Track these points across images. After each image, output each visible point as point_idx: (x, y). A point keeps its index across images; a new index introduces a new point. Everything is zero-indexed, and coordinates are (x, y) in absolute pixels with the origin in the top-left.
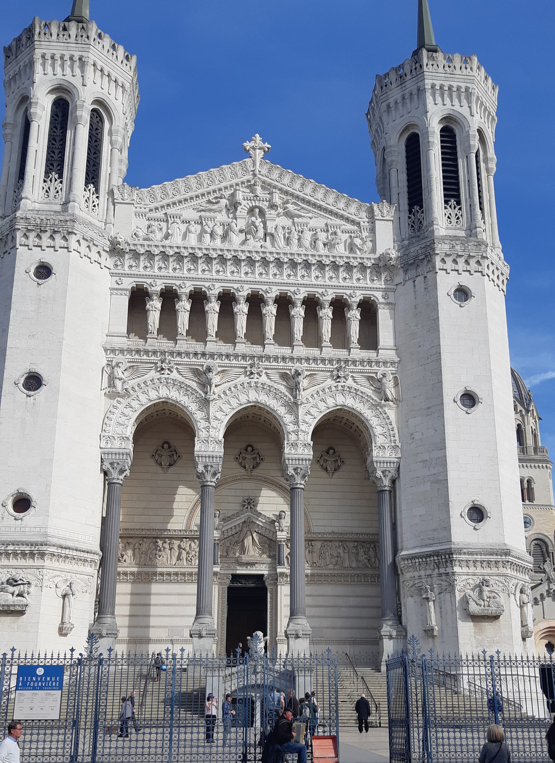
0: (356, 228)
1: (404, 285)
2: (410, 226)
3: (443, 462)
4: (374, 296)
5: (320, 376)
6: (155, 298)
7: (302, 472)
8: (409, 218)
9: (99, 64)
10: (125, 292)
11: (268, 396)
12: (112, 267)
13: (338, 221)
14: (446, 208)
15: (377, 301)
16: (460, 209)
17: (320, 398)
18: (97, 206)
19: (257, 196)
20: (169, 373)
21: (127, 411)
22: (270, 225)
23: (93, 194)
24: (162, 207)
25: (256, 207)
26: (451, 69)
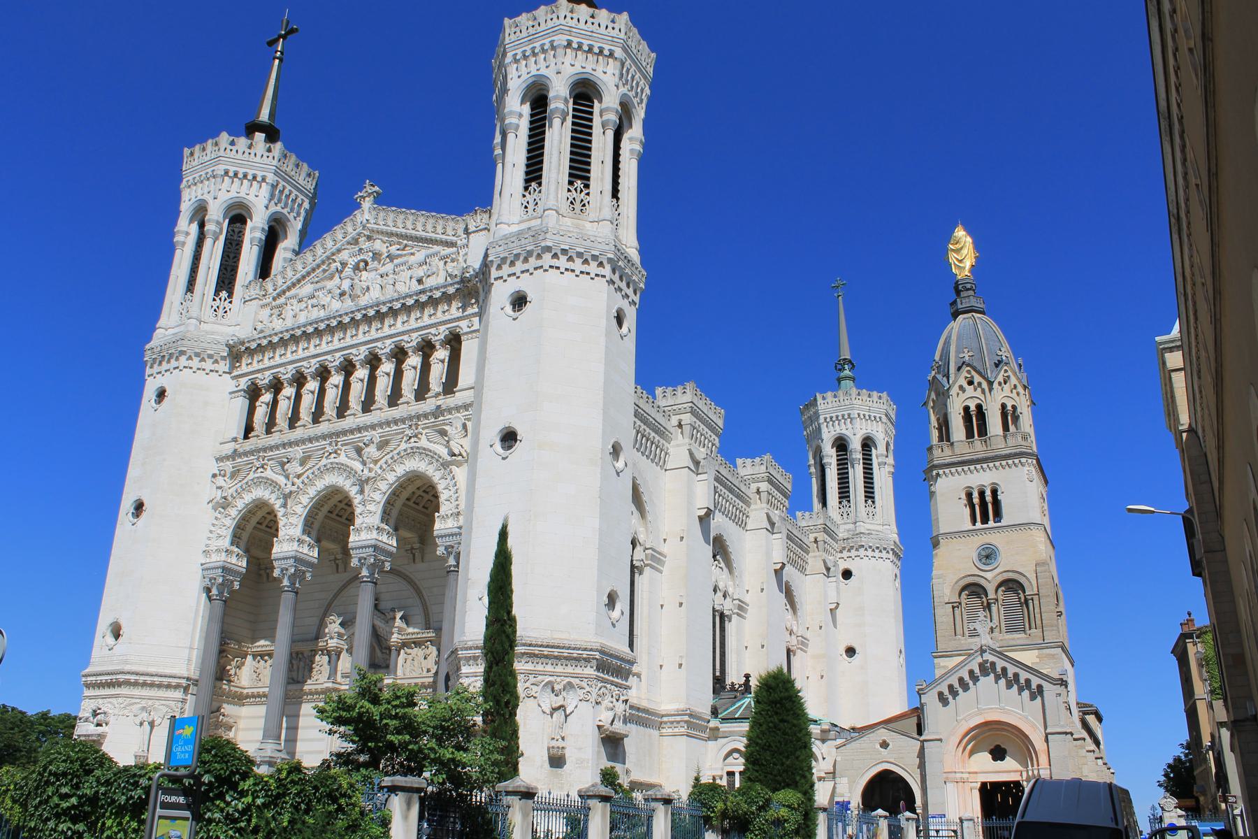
6: (264, 391)
9: (232, 170)
13: (436, 248)
14: (524, 196)
16: (540, 192)
23: (225, 300)
24: (284, 292)
26: (535, 28)
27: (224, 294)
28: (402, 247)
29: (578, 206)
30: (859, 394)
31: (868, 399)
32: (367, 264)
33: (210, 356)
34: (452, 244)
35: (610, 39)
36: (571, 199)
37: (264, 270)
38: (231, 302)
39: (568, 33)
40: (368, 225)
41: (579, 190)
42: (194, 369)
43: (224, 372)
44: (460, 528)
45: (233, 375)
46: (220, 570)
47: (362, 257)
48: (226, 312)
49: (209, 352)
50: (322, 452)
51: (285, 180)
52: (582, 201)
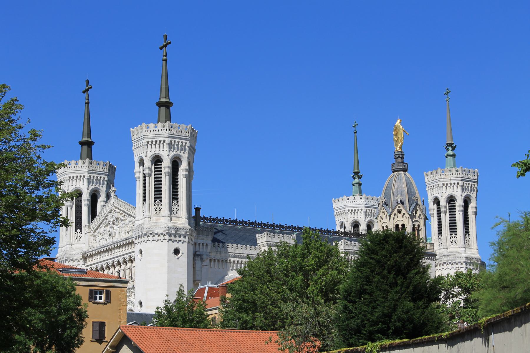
29: (158, 211)
30: (443, 172)
31: (449, 173)
33: (76, 260)
35: (163, 135)
36: (155, 209)
37: (93, 214)
38: (81, 233)
39: (147, 138)
41: (158, 204)
43: (82, 265)
45: (86, 265)
48: (80, 238)
49: (75, 258)
51: (93, 173)
52: (159, 208)
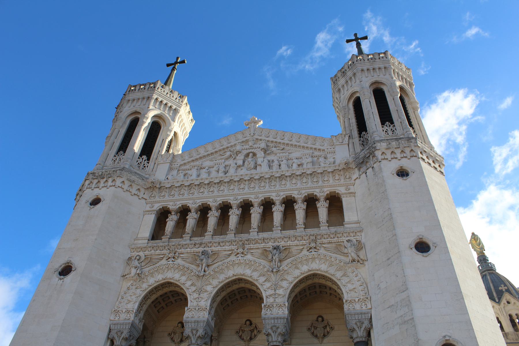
0: (321, 153)
1: (360, 178)
2: (361, 144)
3: (408, 303)
4: (338, 190)
5: (294, 250)
6: (173, 213)
7: (279, 330)
8: (360, 140)
10: (154, 212)
11: (250, 269)
12: (148, 198)
14: (383, 127)
15: (340, 192)
16: (394, 126)
17: (294, 266)
18: (146, 167)
19: (251, 146)
20: (173, 260)
21: (138, 291)
22: (259, 161)
23: (145, 161)
24: (189, 162)
25: (251, 152)
26: (373, 60)
27: (145, 157)
28: (282, 149)
32: (254, 155)
34: (319, 150)
38: (148, 163)
40: (254, 137)
42: (125, 190)
44: (371, 309)
46: (128, 327)
47: (251, 150)
48: (145, 167)
50: (230, 252)
